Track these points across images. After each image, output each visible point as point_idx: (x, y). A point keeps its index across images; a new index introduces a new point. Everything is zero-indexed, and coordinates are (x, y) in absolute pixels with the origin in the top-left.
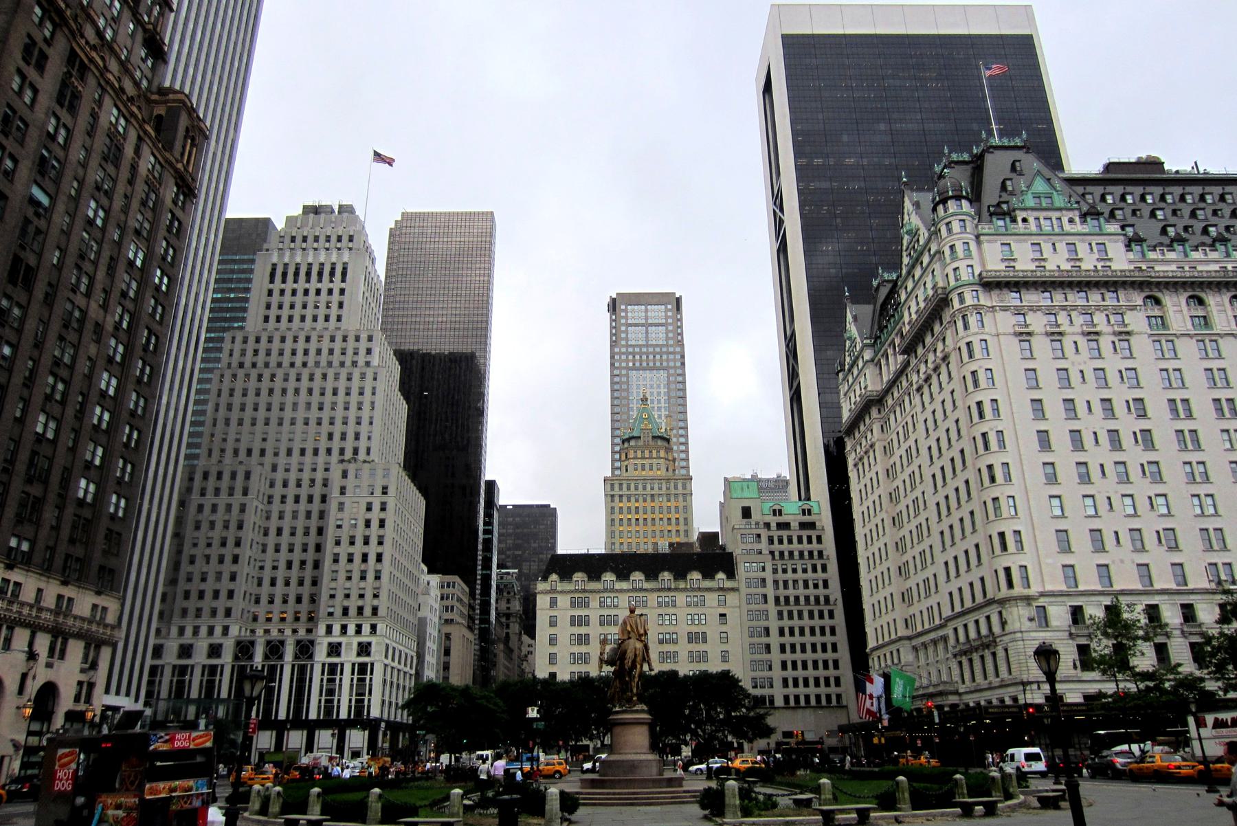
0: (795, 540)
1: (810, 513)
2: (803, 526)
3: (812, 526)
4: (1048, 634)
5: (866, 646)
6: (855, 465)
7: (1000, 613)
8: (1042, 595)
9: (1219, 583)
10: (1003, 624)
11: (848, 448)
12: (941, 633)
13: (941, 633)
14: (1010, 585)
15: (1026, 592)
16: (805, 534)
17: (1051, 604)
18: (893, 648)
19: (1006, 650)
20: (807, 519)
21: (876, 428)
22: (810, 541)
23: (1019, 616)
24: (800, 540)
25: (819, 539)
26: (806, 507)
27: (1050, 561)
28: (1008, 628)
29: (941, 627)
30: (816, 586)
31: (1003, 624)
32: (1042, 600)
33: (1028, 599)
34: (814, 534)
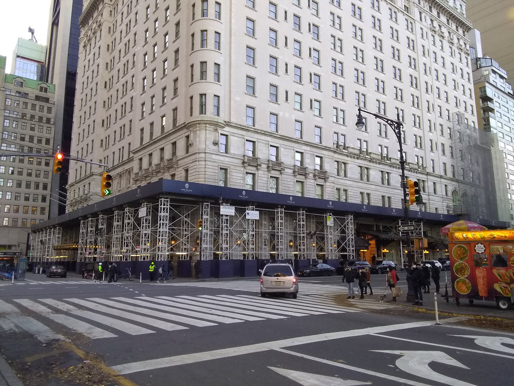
0: (30, 106)
1: (46, 91)
2: (37, 98)
3: (47, 100)
4: (227, 159)
5: (66, 183)
6: (85, 47)
7: (188, 137)
8: (228, 124)
9: (338, 146)
10: (188, 146)
11: (82, 35)
12: (127, 167)
13: (127, 167)
14: (203, 110)
15: (216, 119)
16: (38, 103)
17: (234, 134)
18: (87, 181)
19: (187, 171)
20: (43, 94)
21: (106, 12)
22: (42, 108)
23: (204, 138)
24: (34, 106)
25: (49, 110)
26: (44, 85)
27: (238, 99)
28: (191, 150)
29: (130, 160)
30: (40, 141)
31: (188, 146)
32: (227, 129)
33: (216, 125)
34: (46, 105)
